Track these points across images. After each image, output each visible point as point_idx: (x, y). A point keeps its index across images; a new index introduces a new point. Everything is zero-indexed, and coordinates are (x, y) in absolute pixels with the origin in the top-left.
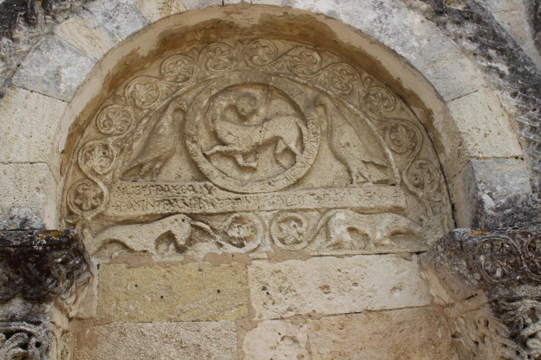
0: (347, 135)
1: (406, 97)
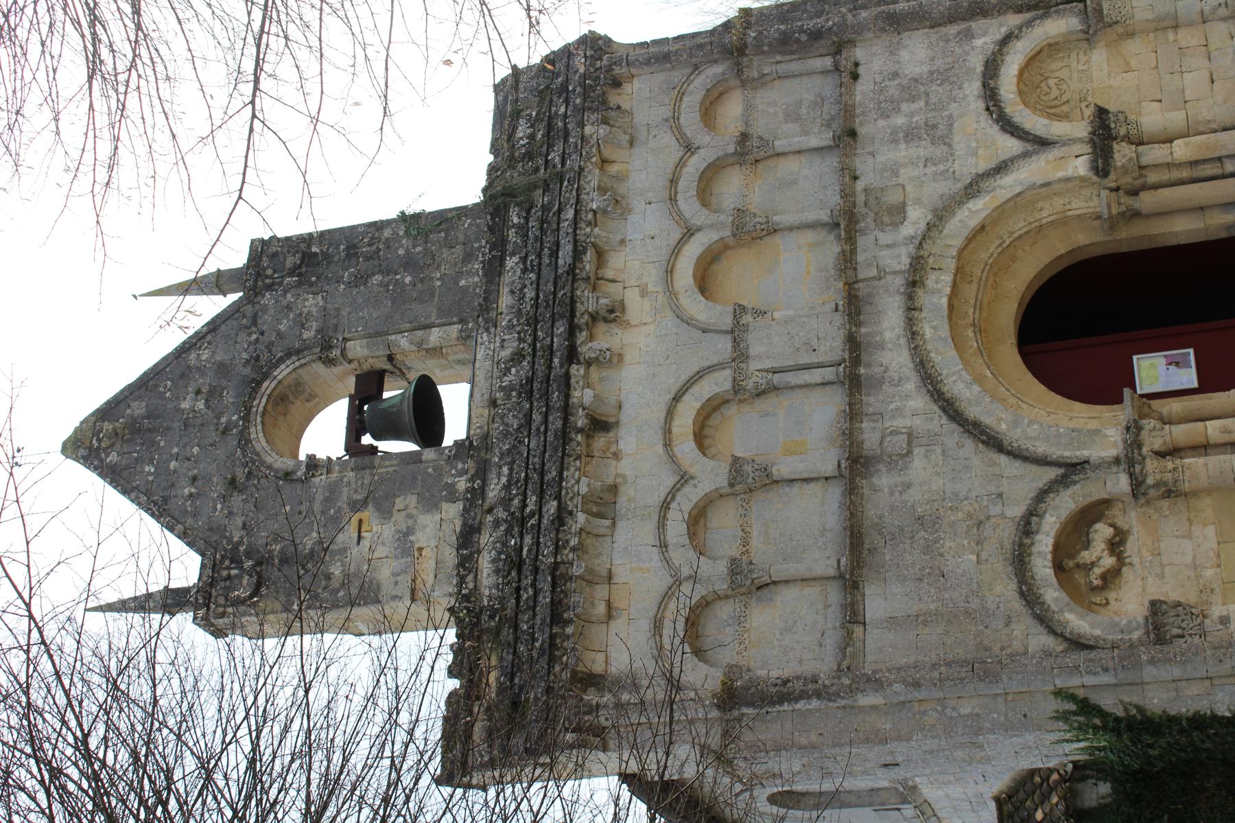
0: (1054, 66)
1: (1039, 52)
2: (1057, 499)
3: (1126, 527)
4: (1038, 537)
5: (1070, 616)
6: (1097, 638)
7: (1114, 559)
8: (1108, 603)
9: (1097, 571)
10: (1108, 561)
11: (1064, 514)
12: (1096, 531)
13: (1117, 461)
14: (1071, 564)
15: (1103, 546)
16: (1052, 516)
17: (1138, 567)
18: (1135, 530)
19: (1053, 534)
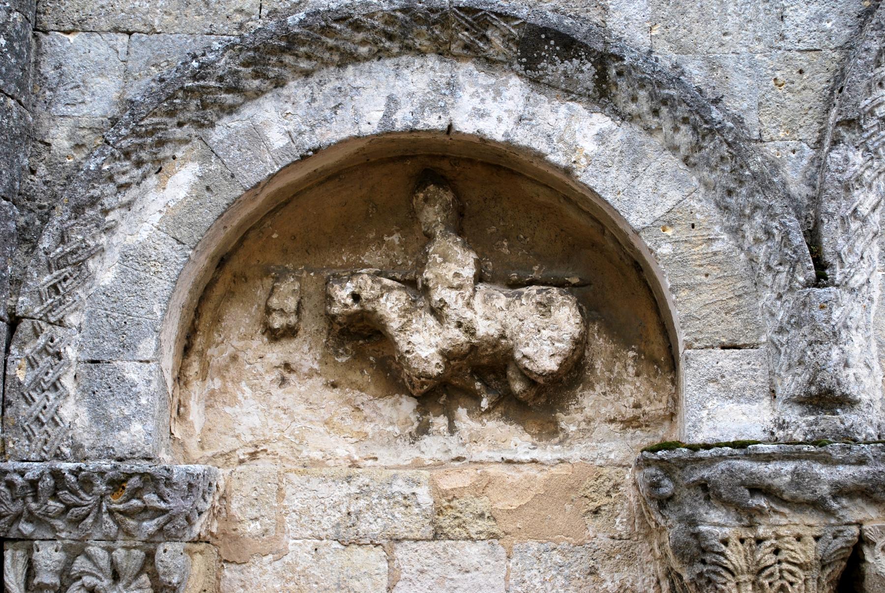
2: (673, 163)
3: (569, 422)
4: (515, 88)
5: (183, 179)
6: (75, 263)
7: (435, 367)
8: (275, 336)
9: (391, 306)
10: (424, 344)
11: (606, 182)
12: (545, 308)
13: (824, 399)
14: (432, 215)
15: (485, 329)
16: (601, 138)
17: (408, 454)
18: (548, 453)
19: (522, 137)
